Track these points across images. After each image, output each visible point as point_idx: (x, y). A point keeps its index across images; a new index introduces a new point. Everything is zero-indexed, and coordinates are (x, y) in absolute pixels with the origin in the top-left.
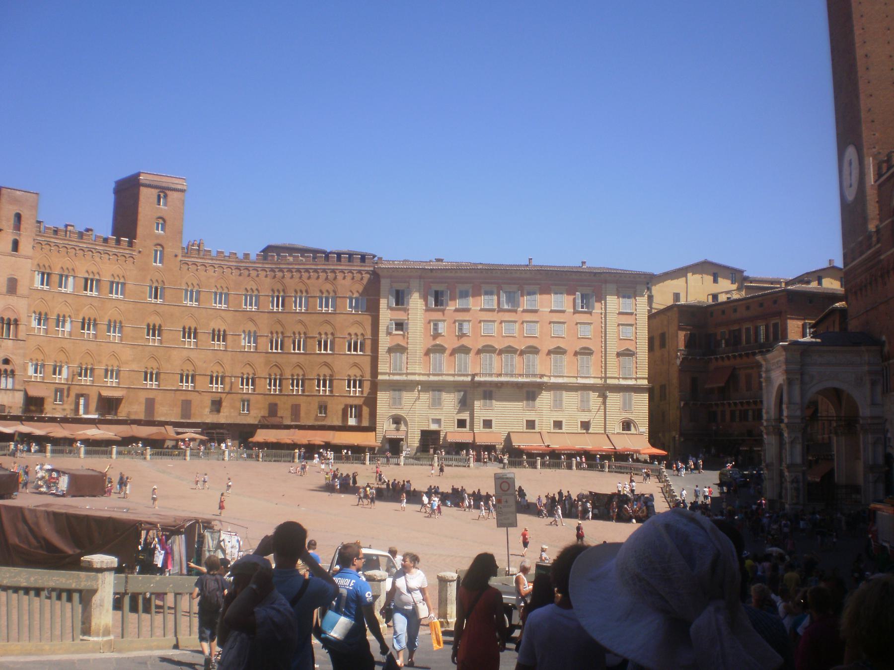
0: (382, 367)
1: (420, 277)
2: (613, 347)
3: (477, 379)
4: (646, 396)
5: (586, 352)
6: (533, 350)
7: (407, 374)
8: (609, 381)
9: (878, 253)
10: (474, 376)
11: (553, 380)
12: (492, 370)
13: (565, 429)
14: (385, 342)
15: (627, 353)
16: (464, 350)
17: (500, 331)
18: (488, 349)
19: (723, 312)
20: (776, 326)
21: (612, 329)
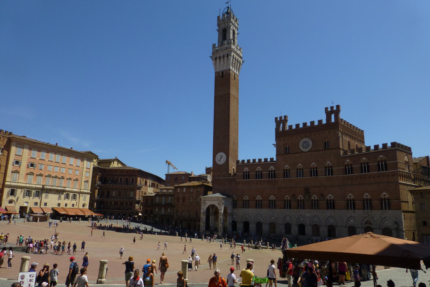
0: (8, 179)
1: (28, 144)
2: (83, 180)
3: (45, 187)
4: (89, 195)
5: (77, 180)
6: (63, 178)
7: (18, 183)
8: (82, 190)
9: (236, 179)
10: (43, 186)
11: (67, 189)
12: (50, 183)
13: (68, 207)
14: (10, 168)
15: (87, 182)
16: (41, 175)
17: (53, 169)
18: (49, 176)
19: (111, 171)
20: (133, 179)
21: (84, 173)
